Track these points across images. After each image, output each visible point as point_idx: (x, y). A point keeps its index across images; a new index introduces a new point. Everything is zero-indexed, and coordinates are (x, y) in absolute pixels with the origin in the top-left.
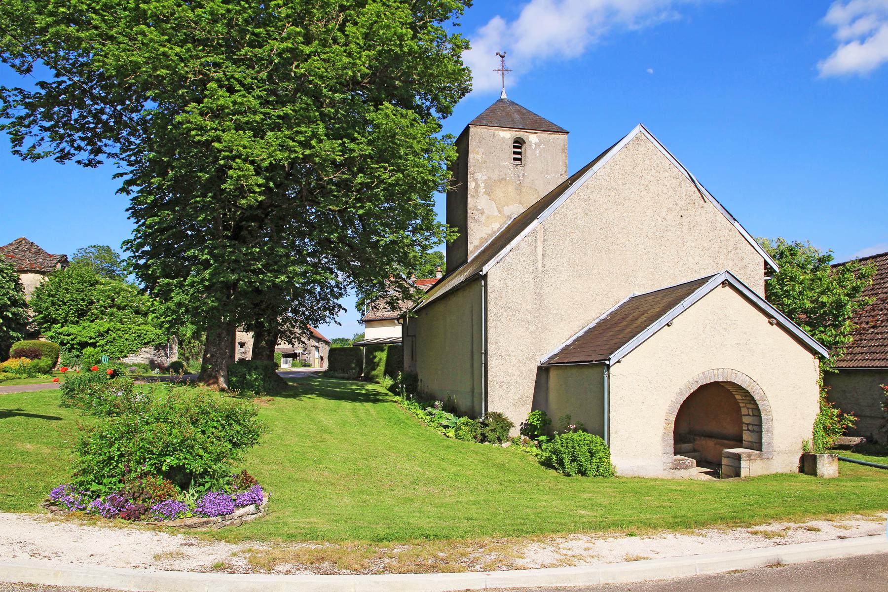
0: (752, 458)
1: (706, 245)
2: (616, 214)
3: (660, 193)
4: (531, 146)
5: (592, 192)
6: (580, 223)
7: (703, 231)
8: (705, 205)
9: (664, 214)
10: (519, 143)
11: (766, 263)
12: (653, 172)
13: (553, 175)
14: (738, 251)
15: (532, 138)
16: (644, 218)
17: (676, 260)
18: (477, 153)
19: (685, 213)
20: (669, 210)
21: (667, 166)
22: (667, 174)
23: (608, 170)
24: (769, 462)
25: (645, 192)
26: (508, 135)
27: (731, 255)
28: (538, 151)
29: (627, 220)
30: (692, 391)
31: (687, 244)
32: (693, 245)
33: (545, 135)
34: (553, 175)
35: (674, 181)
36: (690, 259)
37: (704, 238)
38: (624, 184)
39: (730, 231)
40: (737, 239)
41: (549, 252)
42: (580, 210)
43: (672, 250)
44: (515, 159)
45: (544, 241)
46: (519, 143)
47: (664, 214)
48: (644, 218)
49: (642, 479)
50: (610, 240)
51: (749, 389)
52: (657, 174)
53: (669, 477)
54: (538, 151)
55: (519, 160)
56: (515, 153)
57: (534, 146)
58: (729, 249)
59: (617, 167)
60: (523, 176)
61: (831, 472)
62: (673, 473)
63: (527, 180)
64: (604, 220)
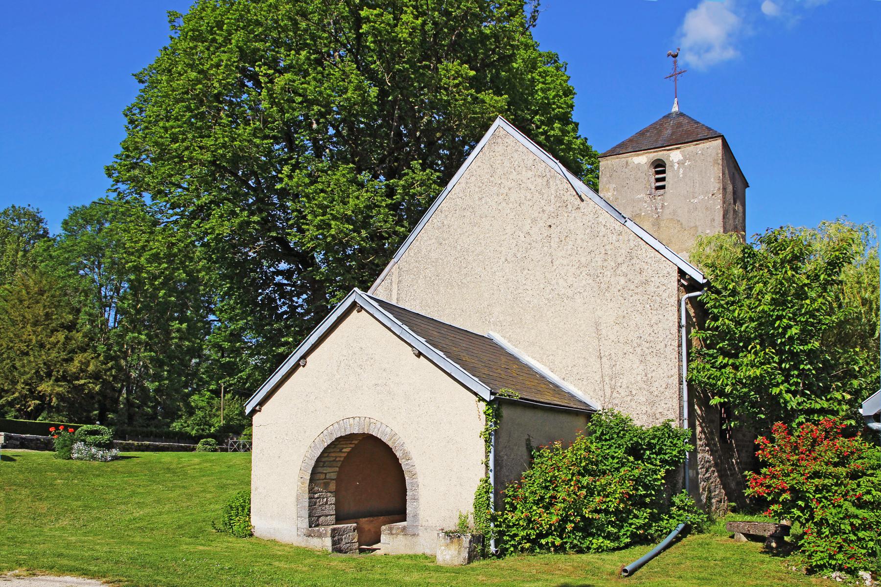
0: (394, 532)
1: (583, 260)
2: (471, 238)
3: (523, 200)
4: (672, 166)
5: (446, 216)
6: (434, 255)
7: (579, 241)
8: (582, 205)
9: (527, 227)
10: (659, 166)
11: (682, 273)
12: (514, 175)
13: (701, 197)
14: (633, 261)
15: (674, 156)
16: (503, 238)
17: (542, 286)
18: (608, 190)
19: (554, 221)
20: (534, 220)
21: (530, 163)
22: (530, 174)
23: (463, 185)
24: (415, 539)
25: (504, 204)
26: (643, 159)
27: (624, 268)
28: (681, 171)
29: (483, 243)
30: (326, 445)
31: (556, 263)
32: (565, 262)
33: (690, 148)
34: (701, 197)
35: (539, 180)
36: (561, 282)
37: (581, 251)
38: (480, 199)
39: (620, 234)
40: (632, 244)
41: (403, 295)
42: (434, 241)
43: (538, 273)
44: (658, 188)
45: (399, 282)
46: (659, 166)
47: (527, 227)
48: (503, 238)
49: (274, 542)
50: (464, 271)
51: (390, 444)
52: (519, 177)
53: (303, 545)
54: (681, 171)
55: (663, 187)
56: (658, 180)
57: (676, 166)
58: (620, 260)
59: (473, 179)
60: (663, 207)
61: (448, 557)
62: (307, 541)
63: (667, 211)
64: (459, 248)
